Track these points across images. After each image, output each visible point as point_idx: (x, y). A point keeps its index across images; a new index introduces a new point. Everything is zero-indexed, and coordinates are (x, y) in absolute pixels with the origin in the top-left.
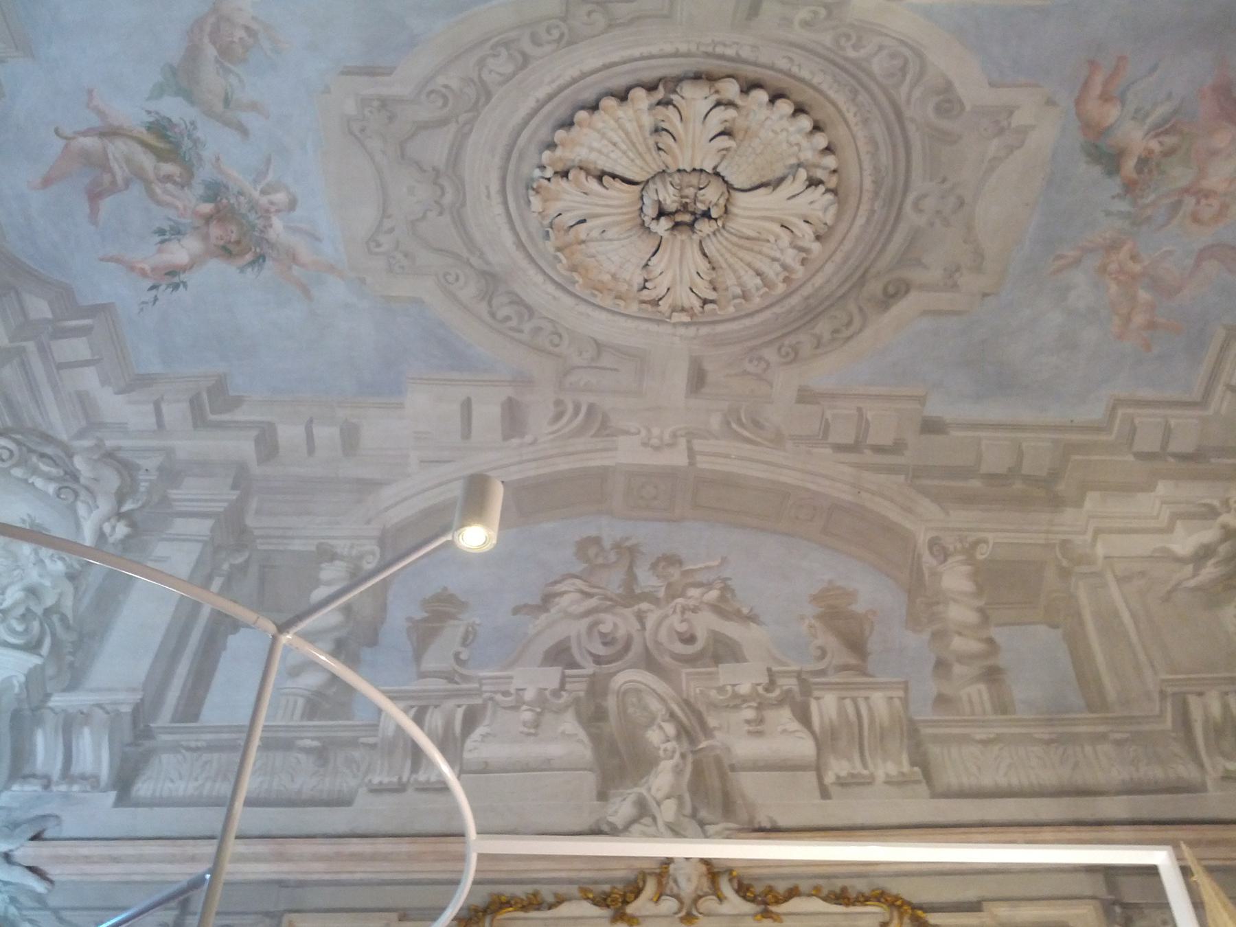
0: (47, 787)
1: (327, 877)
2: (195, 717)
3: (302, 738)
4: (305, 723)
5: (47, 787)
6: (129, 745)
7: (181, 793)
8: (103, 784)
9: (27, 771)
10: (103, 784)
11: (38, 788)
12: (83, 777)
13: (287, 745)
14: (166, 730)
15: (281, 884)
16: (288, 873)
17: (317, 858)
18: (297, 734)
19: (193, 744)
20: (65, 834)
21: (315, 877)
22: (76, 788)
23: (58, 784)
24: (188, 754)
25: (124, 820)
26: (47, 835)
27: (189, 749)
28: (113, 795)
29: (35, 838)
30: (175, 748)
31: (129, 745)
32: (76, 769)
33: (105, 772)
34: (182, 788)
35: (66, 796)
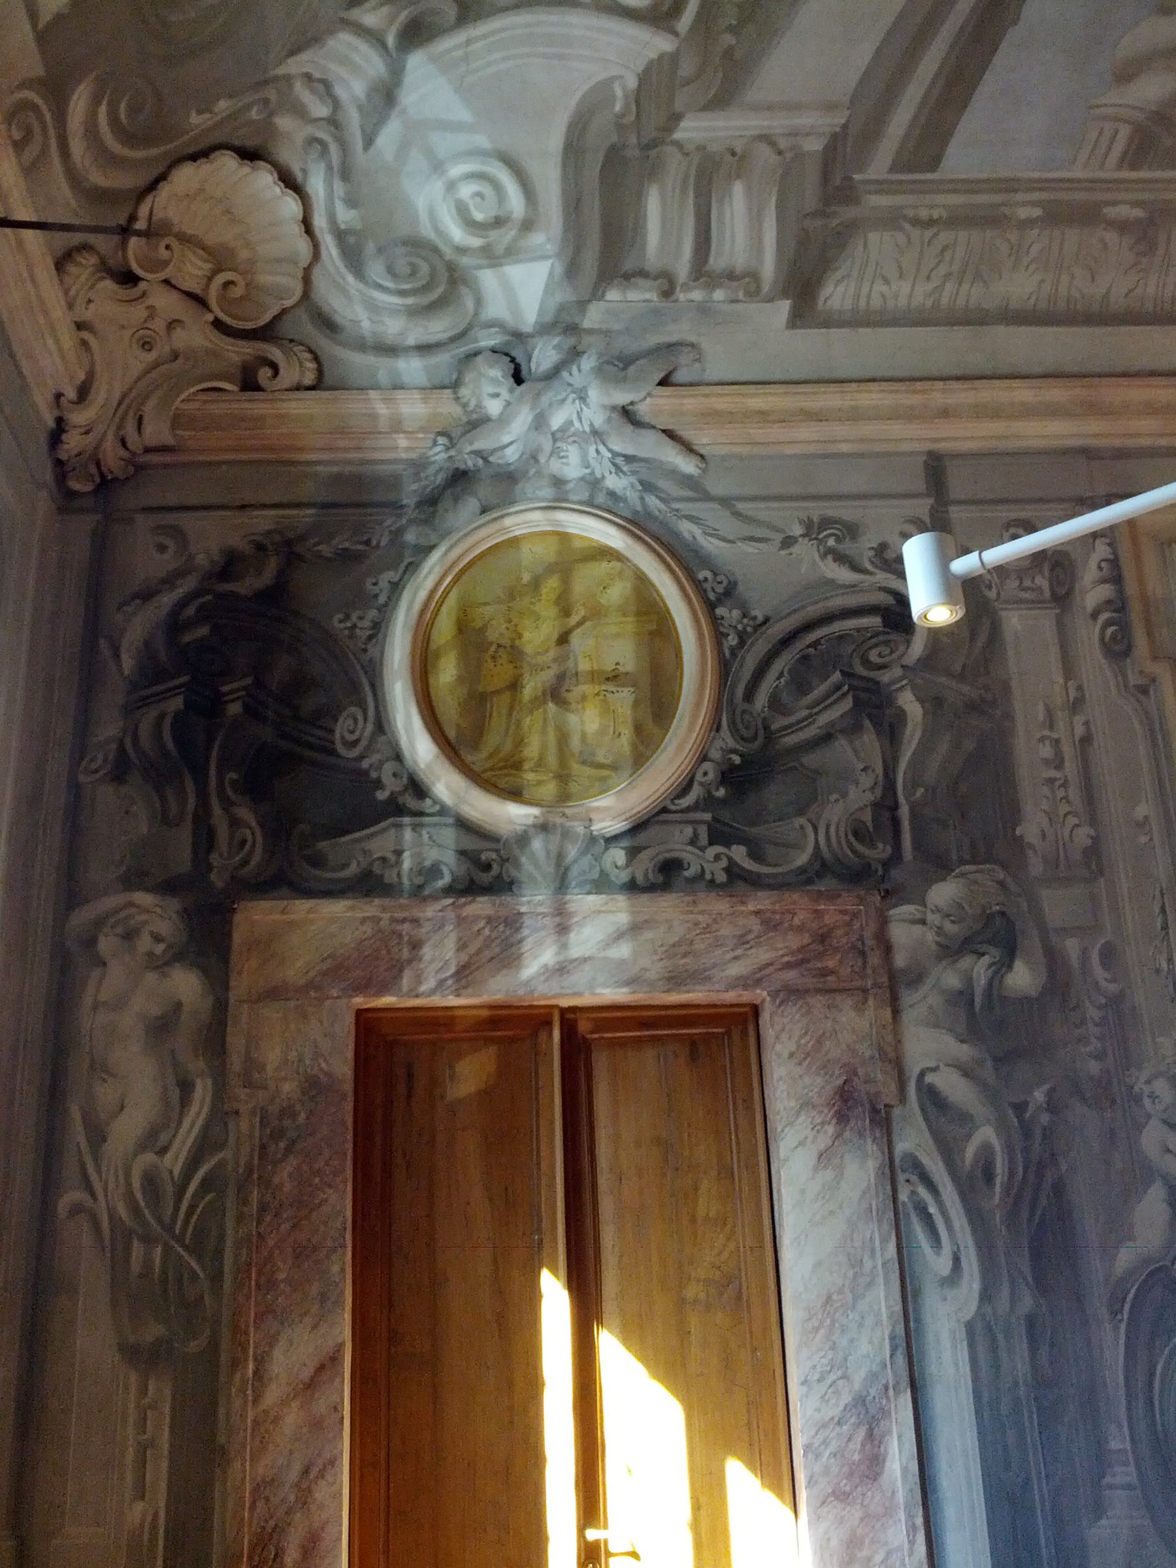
0: (667, 293)
1: (1163, 442)
2: (935, 163)
3: (1115, 203)
4: (1125, 174)
5: (667, 293)
6: (815, 214)
7: (902, 302)
8: (766, 288)
9: (628, 265)
10: (766, 288)
11: (653, 296)
12: (731, 276)
13: (1087, 216)
14: (882, 187)
15: (1088, 453)
16: (1095, 436)
17: (1150, 409)
18: (1108, 196)
19: (924, 214)
20: (710, 376)
21: (1145, 442)
22: (719, 295)
23: (686, 287)
24: (916, 233)
25: (809, 348)
26: (680, 376)
27: (916, 222)
28: (785, 306)
29: (663, 383)
30: (892, 221)
31: (815, 214)
32: (717, 262)
33: (768, 269)
34: (904, 293)
35: (704, 310)
